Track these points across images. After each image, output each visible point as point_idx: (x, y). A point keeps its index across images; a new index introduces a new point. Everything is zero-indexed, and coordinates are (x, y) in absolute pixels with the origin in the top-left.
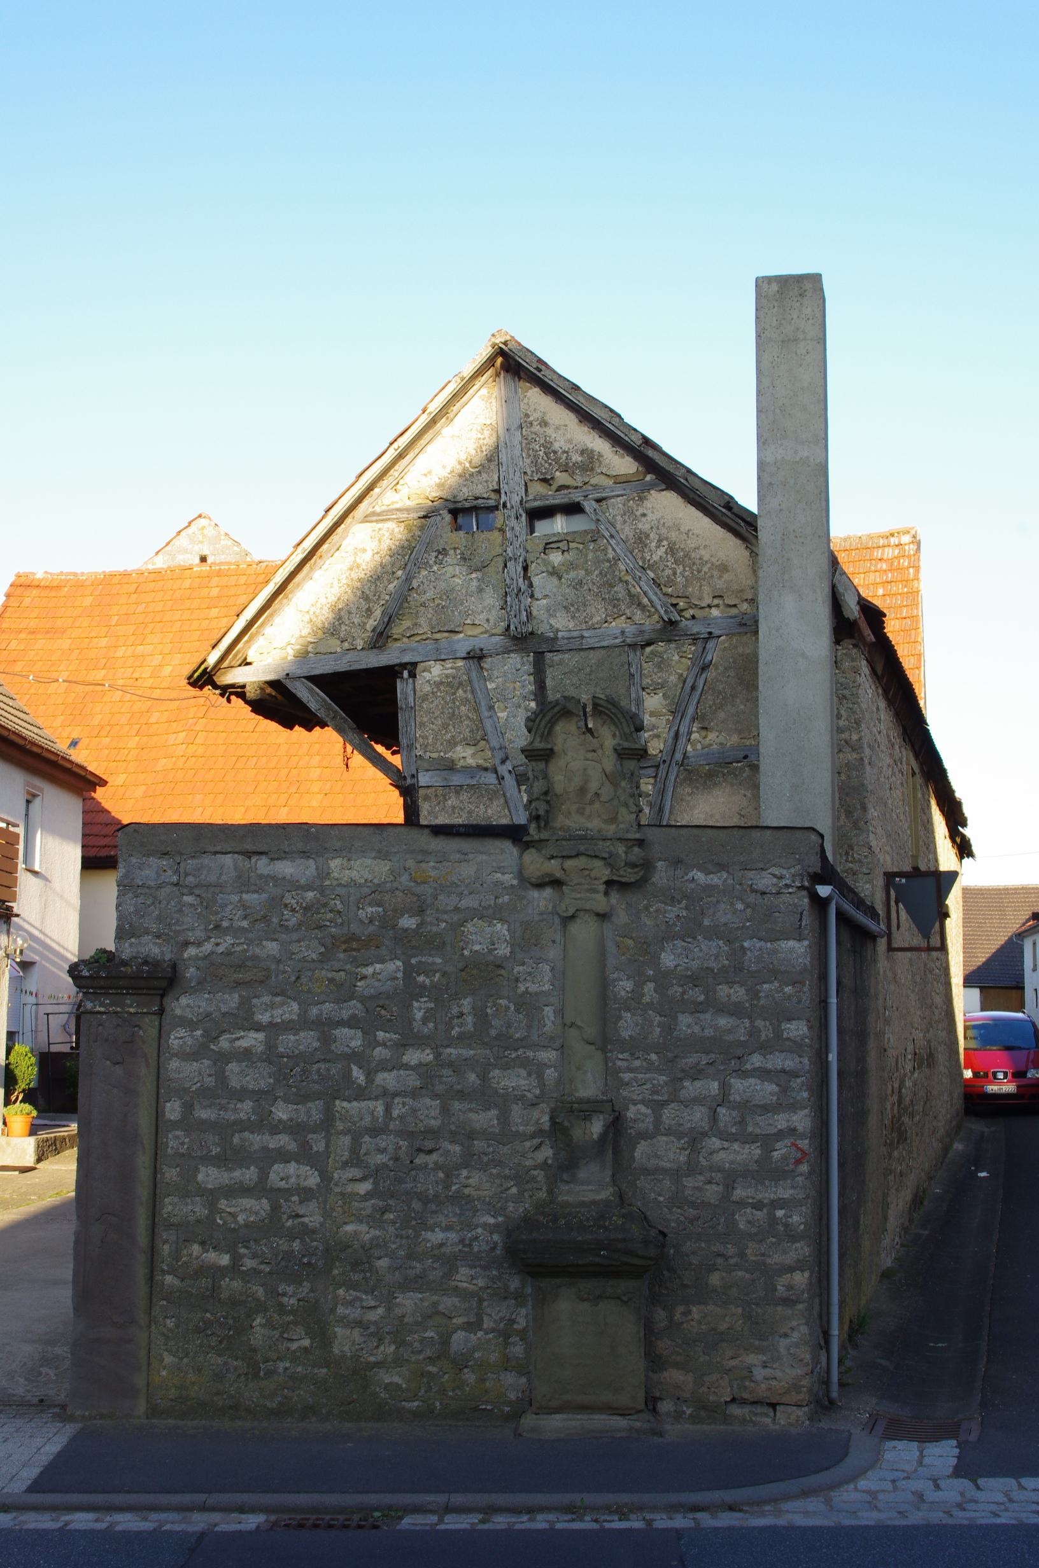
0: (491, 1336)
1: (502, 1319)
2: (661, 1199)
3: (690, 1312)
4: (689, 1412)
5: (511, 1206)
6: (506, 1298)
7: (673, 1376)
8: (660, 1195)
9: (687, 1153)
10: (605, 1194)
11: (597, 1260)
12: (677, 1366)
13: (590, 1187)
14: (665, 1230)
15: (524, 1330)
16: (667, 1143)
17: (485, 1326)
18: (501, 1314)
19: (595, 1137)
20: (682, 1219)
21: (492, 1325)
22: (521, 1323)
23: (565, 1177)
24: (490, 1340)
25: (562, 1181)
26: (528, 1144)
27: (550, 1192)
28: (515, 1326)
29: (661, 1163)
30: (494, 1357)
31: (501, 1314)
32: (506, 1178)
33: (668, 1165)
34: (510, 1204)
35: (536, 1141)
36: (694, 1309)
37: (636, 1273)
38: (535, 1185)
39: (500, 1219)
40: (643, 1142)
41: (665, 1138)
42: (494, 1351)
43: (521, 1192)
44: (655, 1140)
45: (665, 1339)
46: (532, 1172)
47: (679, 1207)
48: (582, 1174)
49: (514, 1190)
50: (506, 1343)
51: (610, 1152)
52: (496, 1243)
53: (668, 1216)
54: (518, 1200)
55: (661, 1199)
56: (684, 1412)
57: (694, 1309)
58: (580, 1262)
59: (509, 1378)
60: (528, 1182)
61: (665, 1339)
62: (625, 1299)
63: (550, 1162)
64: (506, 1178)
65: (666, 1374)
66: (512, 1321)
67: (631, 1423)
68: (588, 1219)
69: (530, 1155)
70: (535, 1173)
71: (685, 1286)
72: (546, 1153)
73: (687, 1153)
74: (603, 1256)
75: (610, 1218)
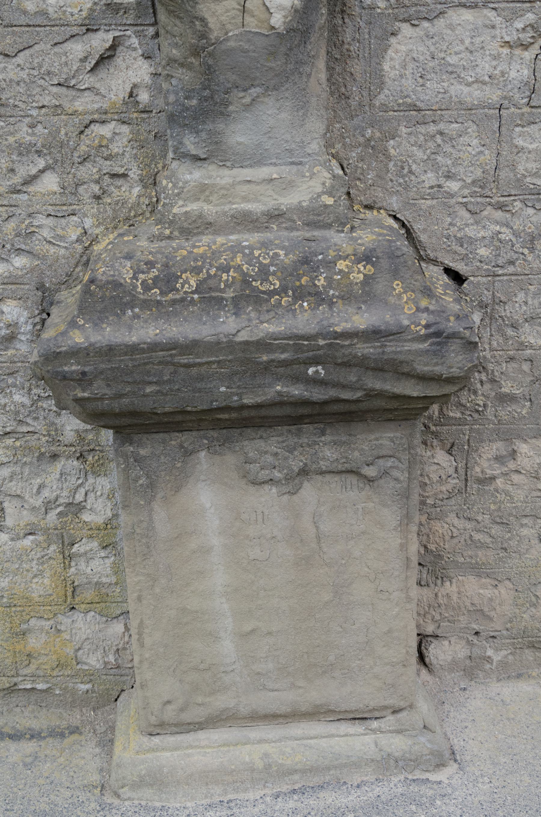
0: (28, 541)
1: (48, 505)
2: (453, 186)
3: (513, 454)
4: (497, 657)
5: (45, 226)
6: (55, 457)
7: (468, 588)
8: (449, 176)
9: (528, 55)
10: (312, 186)
11: (297, 391)
12: (477, 570)
13: (264, 172)
14: (460, 267)
15: (110, 525)
16: (475, 32)
17: (9, 522)
18: (46, 493)
19: (278, 20)
20: (506, 235)
21: (27, 517)
22: (97, 512)
23: (190, 143)
24: (26, 552)
25: (182, 156)
26: (77, 49)
27: (151, 181)
28: (86, 517)
29: (457, 90)
30: (42, 586)
31: (46, 493)
32: (24, 150)
33: (474, 94)
34: (40, 220)
35: (100, 41)
36: (523, 448)
37: (402, 411)
38: (107, 166)
39: (20, 262)
40: (406, 29)
41: (467, 15)
42: (40, 574)
43: (71, 189)
44: (441, 23)
45: (452, 518)
46: (98, 130)
47: (500, 207)
48: (239, 134)
49: (50, 183)
50: (68, 558)
51: (321, 64)
52: (13, 325)
53: (470, 232)
54: (63, 210)
55: (453, 186)
56: (489, 659)
57: (523, 448)
58: (247, 400)
59: (82, 626)
60: (85, 160)
61: (452, 518)
62: (370, 472)
63: (144, 97)
64: (24, 150)
65: (449, 588)
66: (75, 508)
67: (385, 740)
68: (264, 273)
69: (88, 81)
70: (106, 130)
71: (505, 399)
72: (133, 71)
73: (528, 55)
74: (316, 381)
75: (330, 264)
